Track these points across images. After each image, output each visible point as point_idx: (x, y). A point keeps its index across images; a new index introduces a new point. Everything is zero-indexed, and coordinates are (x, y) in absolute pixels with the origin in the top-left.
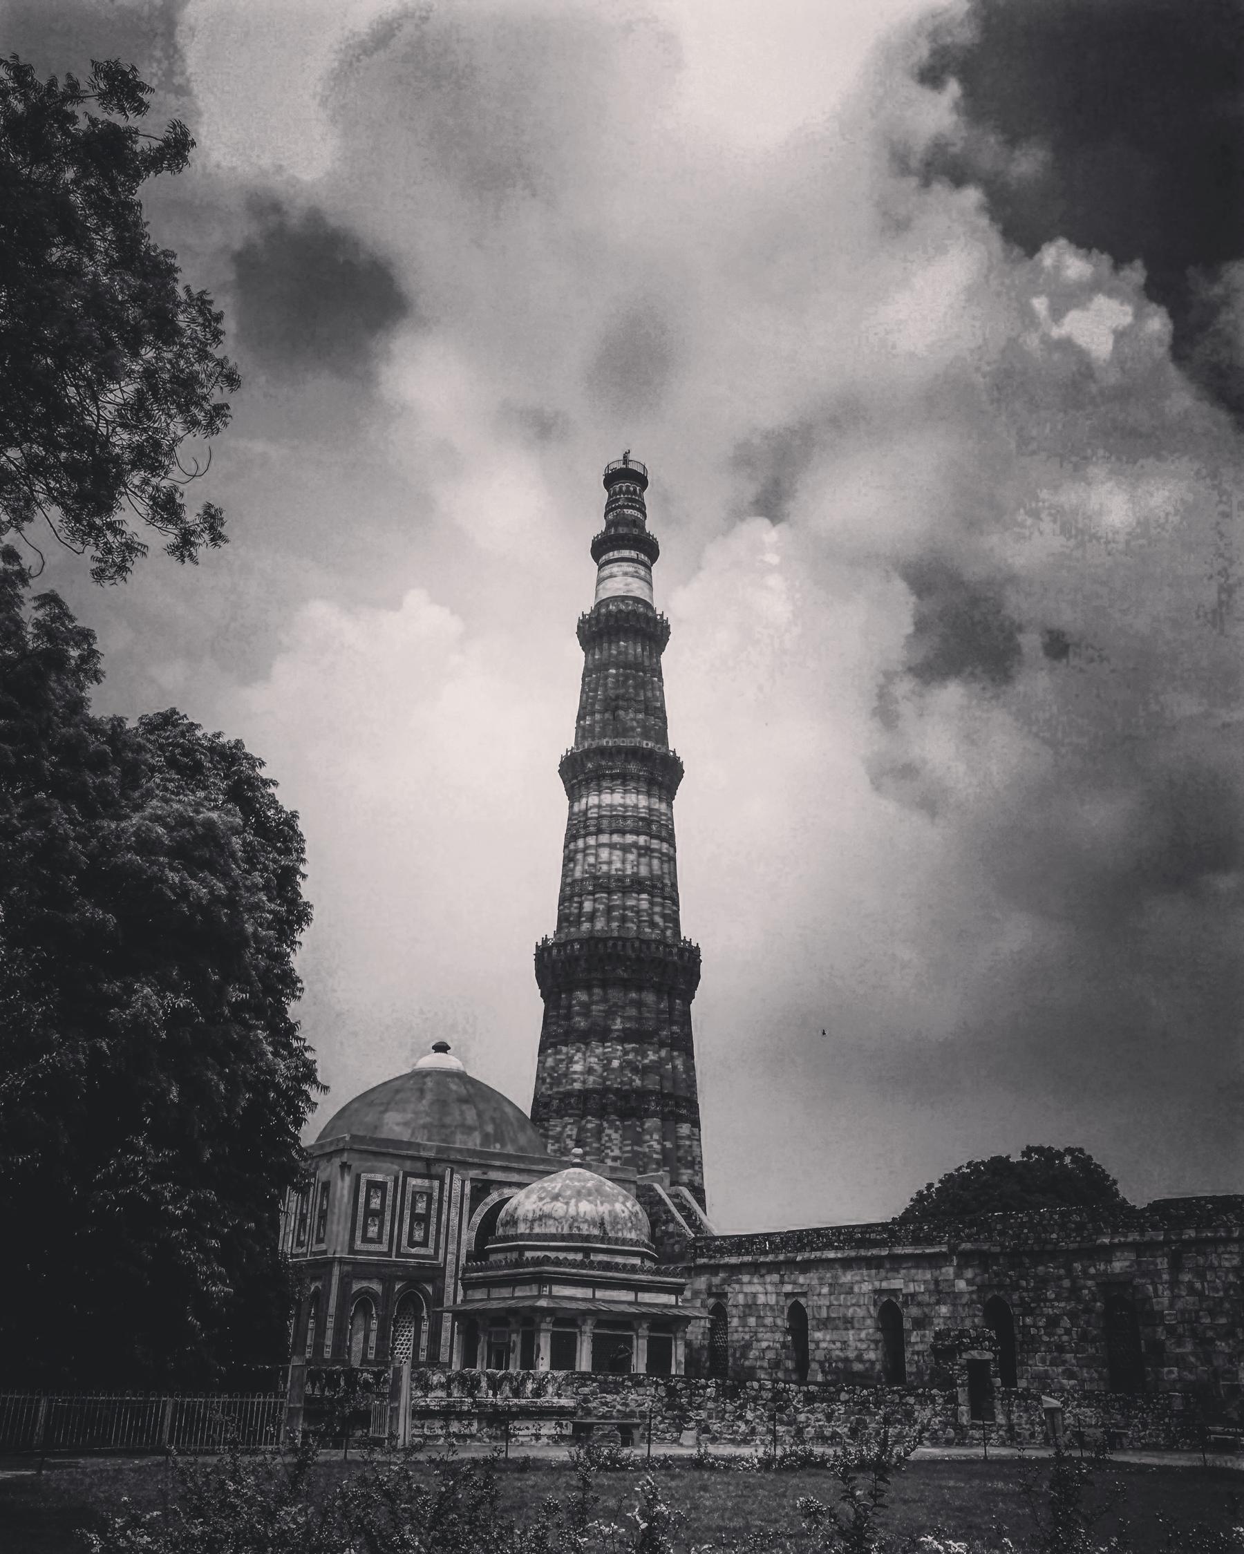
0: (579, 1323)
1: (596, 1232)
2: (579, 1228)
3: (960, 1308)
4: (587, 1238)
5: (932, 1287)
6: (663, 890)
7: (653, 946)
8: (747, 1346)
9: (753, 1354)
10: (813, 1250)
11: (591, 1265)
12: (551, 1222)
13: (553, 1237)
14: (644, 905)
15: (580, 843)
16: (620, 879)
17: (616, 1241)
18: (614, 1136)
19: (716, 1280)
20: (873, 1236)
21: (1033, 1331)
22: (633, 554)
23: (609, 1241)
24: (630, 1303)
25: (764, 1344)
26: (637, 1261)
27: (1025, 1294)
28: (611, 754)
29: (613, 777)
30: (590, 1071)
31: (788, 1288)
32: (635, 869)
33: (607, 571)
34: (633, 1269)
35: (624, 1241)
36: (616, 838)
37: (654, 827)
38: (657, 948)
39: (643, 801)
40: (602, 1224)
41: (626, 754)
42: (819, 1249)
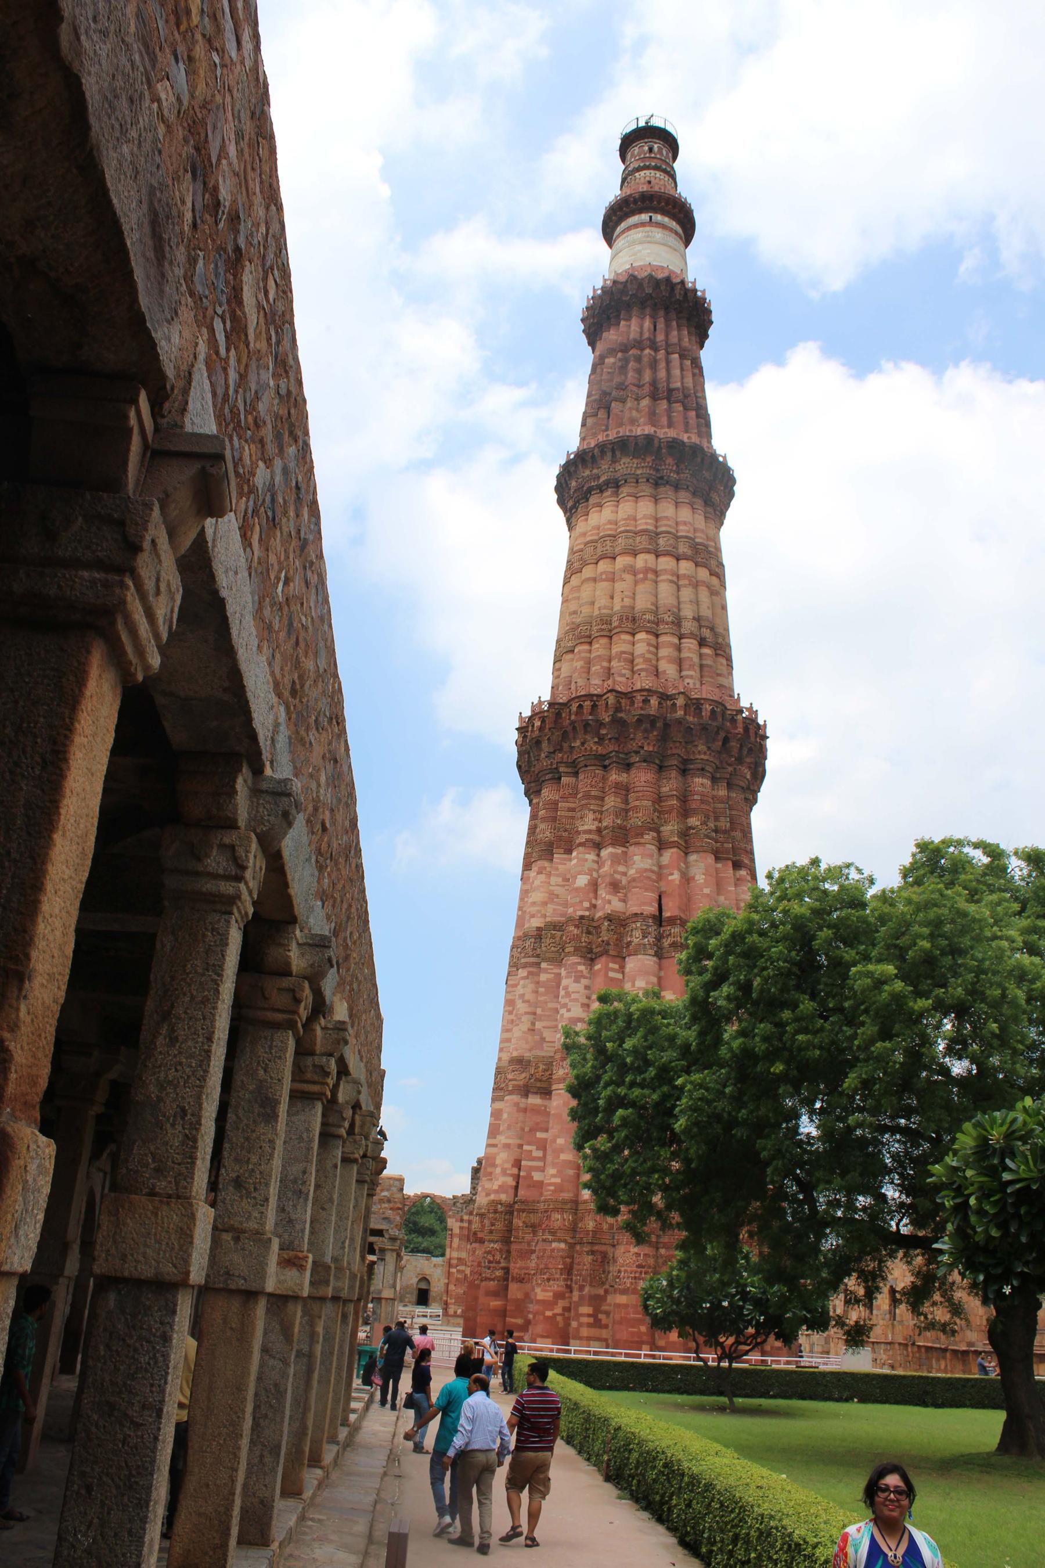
6: (715, 644)
7: (639, 698)
14: (641, 648)
16: (605, 620)
18: (573, 987)
22: (645, 217)
28: (593, 457)
30: (552, 896)
32: (627, 602)
36: (603, 566)
37: (661, 542)
38: (646, 701)
39: (645, 508)
41: (613, 451)
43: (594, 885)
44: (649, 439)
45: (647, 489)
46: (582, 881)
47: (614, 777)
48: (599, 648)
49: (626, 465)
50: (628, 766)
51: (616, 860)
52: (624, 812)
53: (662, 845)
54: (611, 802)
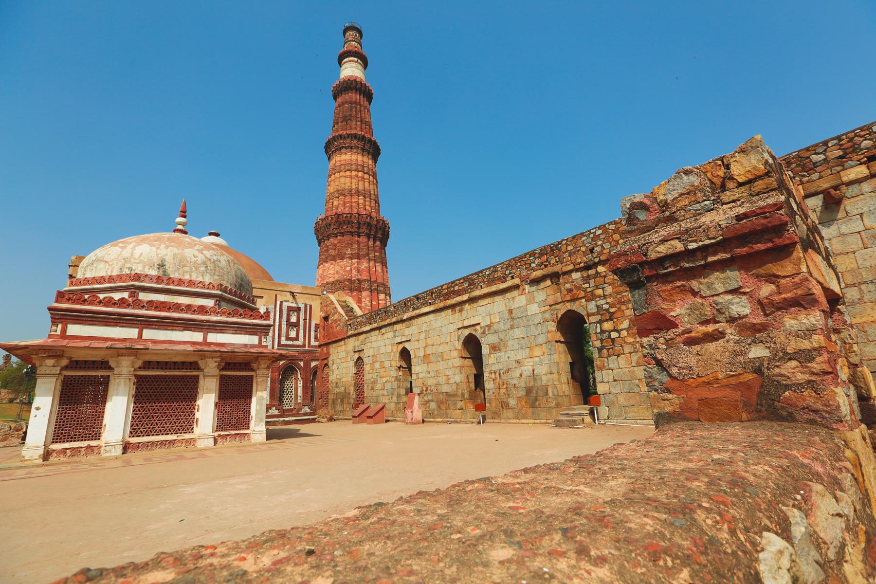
0: (112, 364)
1: (154, 272)
2: (131, 269)
3: (533, 328)
4: (137, 277)
5: (506, 315)
8: (375, 382)
9: (379, 386)
10: (414, 309)
11: (138, 304)
12: (102, 265)
13: (102, 280)
14: (361, 201)
15: (333, 177)
16: (350, 190)
17: (180, 282)
19: (358, 343)
20: (456, 288)
21: (614, 335)
23: (170, 280)
24: (194, 343)
25: (384, 380)
26: (209, 303)
27: (603, 302)
29: (346, 148)
30: (337, 272)
31: (398, 340)
33: (343, 67)
34: (202, 310)
35: (191, 283)
36: (348, 173)
39: (360, 158)
40: (161, 266)
42: (418, 308)
43: (351, 270)
44: (364, 137)
45: (360, 151)
46: (348, 268)
47: (356, 238)
48: (348, 199)
49: (355, 142)
50: (359, 236)
51: (358, 263)
52: (359, 249)
53: (370, 260)
54: (355, 246)
